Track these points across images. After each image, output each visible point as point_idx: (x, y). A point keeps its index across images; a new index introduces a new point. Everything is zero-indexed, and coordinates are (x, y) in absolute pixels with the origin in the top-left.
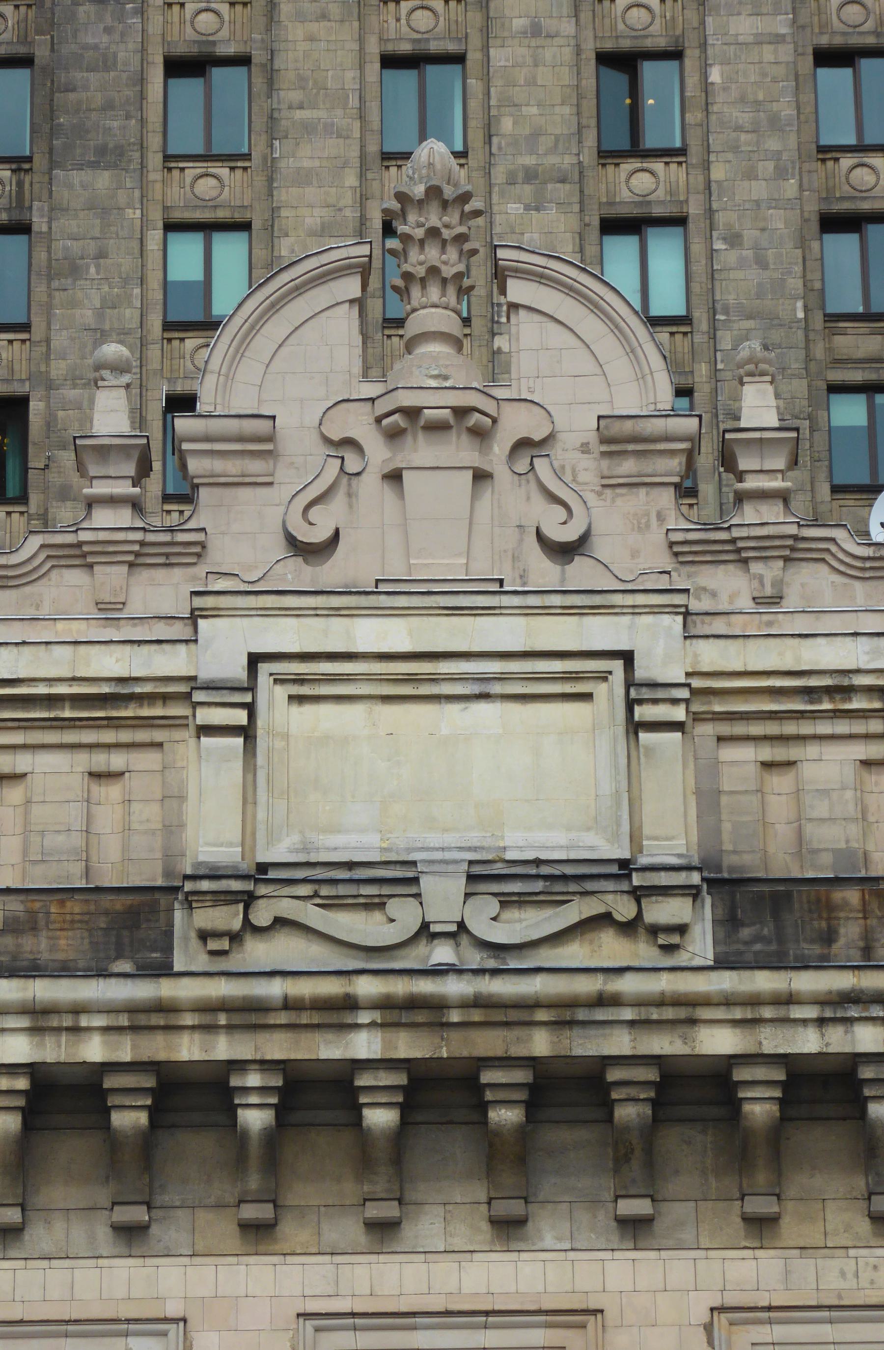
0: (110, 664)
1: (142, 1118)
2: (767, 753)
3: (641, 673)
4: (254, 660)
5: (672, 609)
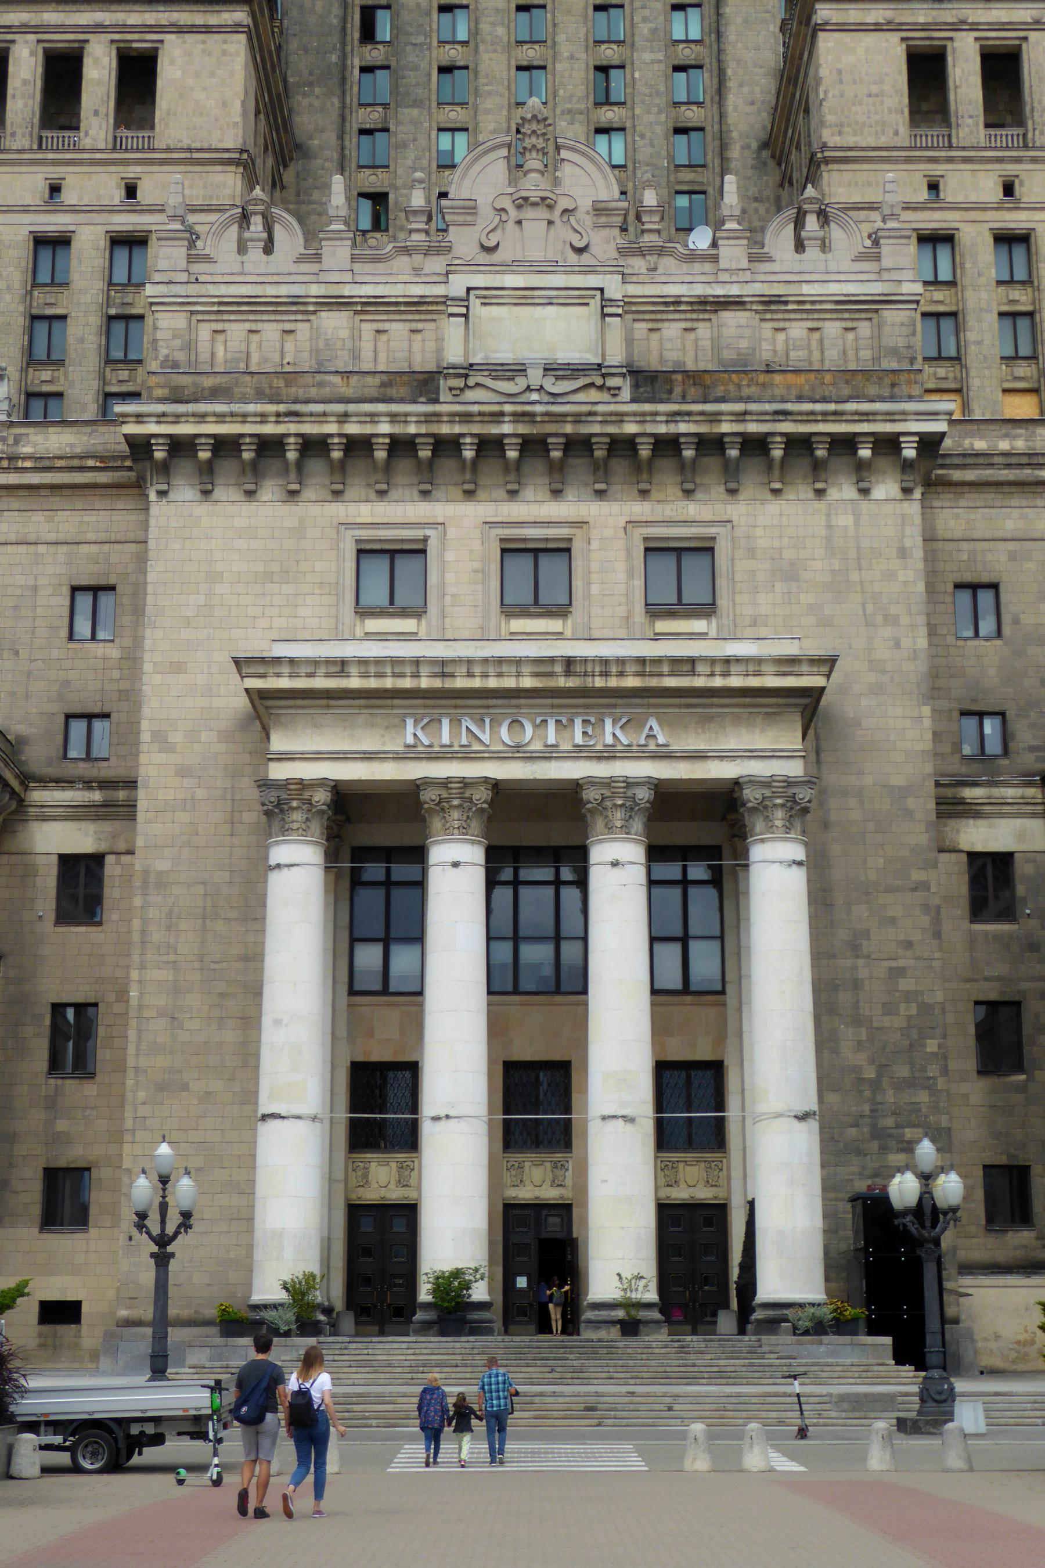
0: (417, 290)
1: (429, 453)
2: (650, 325)
3: (606, 296)
4: (469, 289)
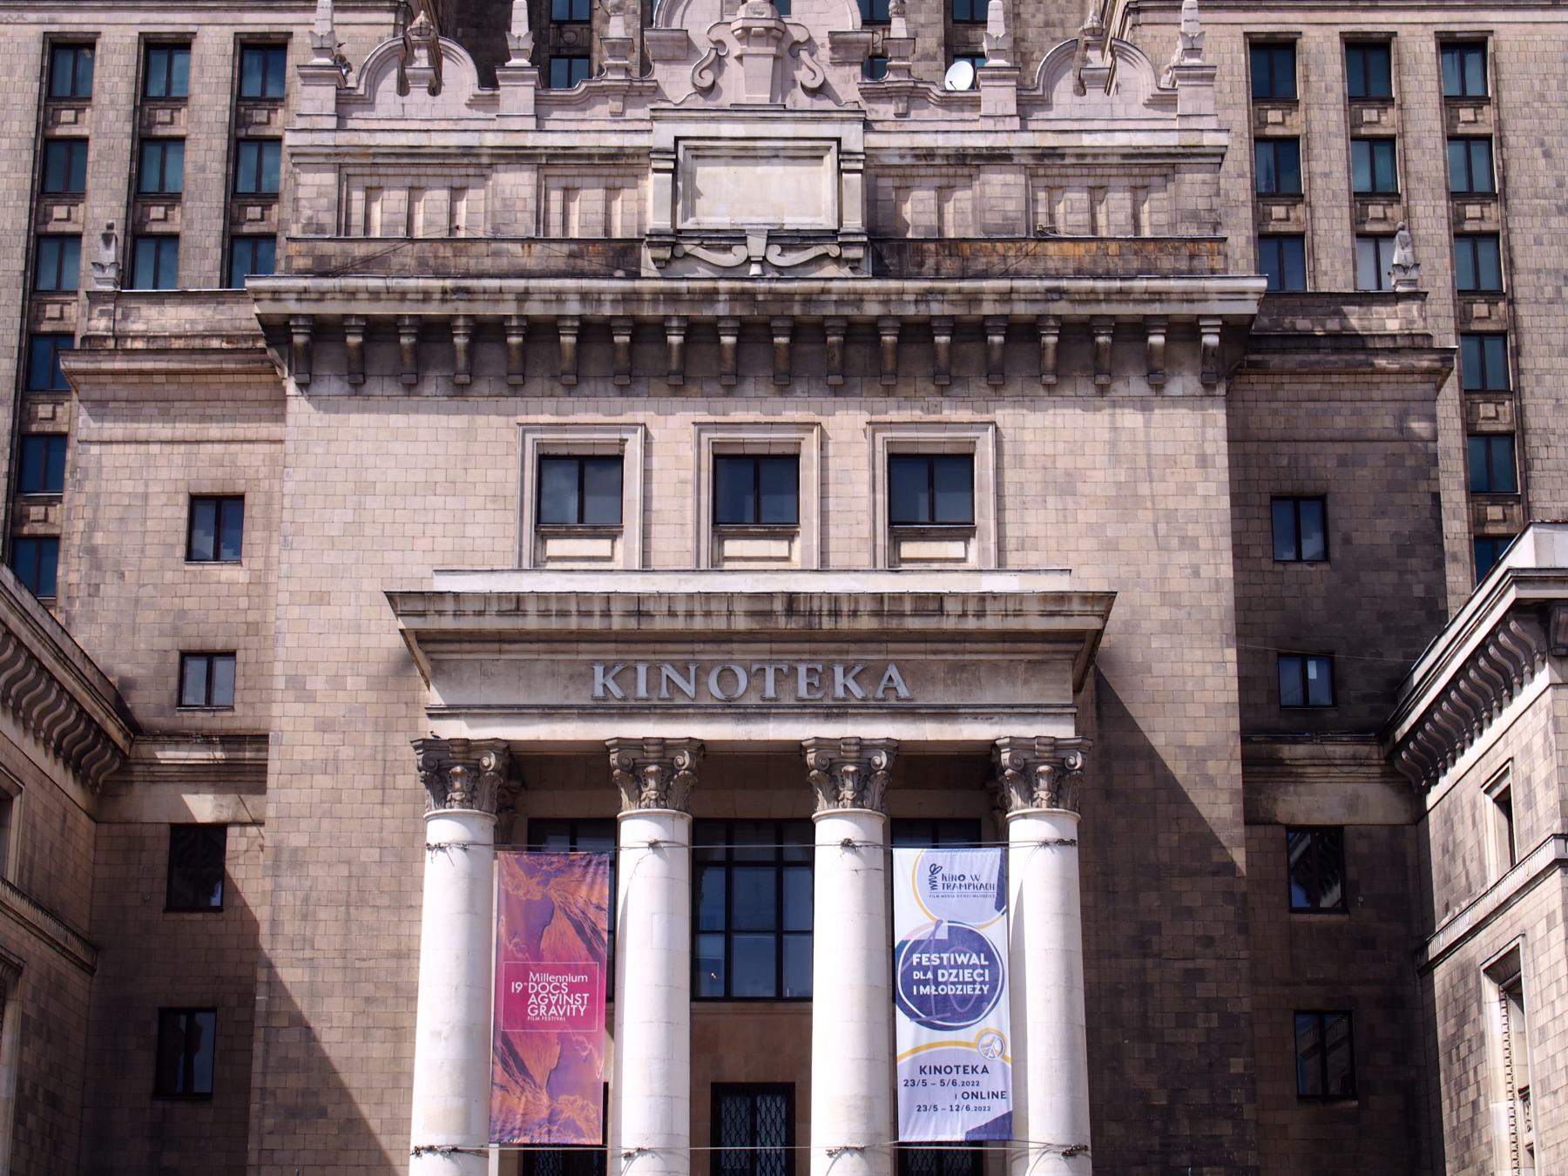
0: (614, 141)
1: (627, 339)
2: (897, 183)
3: (844, 147)
4: (677, 139)
5: (859, 120)
